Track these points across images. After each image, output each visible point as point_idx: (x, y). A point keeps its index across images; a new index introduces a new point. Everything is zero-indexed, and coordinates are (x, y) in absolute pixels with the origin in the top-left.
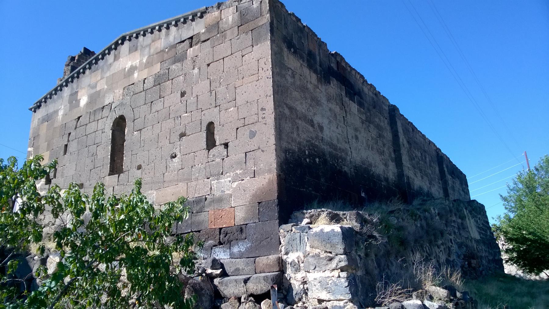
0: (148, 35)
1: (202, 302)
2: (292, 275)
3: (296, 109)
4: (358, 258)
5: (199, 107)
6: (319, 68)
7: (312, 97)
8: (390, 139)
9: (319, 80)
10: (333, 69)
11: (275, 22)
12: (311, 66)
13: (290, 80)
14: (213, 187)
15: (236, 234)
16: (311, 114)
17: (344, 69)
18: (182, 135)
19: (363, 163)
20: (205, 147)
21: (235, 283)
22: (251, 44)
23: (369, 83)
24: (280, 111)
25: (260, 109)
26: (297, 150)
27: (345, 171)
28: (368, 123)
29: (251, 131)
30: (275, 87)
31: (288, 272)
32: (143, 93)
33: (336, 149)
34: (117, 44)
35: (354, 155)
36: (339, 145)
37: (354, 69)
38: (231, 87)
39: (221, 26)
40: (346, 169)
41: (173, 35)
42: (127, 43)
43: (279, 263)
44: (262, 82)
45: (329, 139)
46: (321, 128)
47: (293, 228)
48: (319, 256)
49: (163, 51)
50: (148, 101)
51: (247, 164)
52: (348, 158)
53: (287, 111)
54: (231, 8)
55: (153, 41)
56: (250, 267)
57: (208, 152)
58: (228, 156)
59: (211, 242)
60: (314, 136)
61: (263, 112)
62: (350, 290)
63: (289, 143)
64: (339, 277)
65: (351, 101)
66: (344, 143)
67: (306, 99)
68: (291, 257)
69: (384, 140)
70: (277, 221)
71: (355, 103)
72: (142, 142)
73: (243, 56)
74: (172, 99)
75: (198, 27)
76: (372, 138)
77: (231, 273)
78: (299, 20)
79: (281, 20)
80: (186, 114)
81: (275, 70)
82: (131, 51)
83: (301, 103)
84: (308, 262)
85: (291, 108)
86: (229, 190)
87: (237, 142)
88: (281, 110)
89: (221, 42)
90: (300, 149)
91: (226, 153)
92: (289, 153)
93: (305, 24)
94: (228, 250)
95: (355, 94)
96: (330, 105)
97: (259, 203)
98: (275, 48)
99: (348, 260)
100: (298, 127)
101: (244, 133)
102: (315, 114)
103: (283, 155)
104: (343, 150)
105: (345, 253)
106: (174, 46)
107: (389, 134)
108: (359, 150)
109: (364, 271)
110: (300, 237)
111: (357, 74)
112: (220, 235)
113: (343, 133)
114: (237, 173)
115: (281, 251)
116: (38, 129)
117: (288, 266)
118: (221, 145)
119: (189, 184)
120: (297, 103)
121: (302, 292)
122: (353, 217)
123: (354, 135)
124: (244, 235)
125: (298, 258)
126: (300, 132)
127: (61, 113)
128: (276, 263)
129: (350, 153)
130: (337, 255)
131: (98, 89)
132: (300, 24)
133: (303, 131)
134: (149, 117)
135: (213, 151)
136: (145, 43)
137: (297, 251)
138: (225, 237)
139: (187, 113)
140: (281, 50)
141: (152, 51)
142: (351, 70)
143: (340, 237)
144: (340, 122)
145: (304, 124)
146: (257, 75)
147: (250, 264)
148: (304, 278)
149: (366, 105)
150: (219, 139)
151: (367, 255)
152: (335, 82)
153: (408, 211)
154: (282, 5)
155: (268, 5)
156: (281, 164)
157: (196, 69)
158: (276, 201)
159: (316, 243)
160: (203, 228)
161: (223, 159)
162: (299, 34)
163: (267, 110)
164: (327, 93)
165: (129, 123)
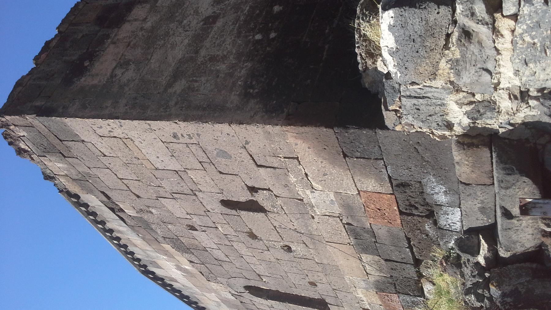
2: (503, 118)
3: (181, 62)
5: (203, 213)
11: (38, 103)
13: (130, 74)
14: (327, 214)
15: (411, 194)
16: (195, 22)
18: (253, 236)
20: (260, 215)
21: (511, 233)
22: (80, 144)
24: (176, 104)
25: (175, 140)
26: (249, 65)
29: (218, 155)
31: (496, 126)
32: (208, 266)
34: (156, 278)
38: (158, 174)
39: (76, 177)
41: (118, 227)
42: (151, 268)
43: (470, 146)
44: (133, 134)
47: (390, 108)
48: (457, 61)
49: (144, 239)
50: (216, 262)
51: (276, 165)
53: (179, 86)
54: (46, 163)
55: (136, 246)
56: (479, 193)
57: (269, 212)
58: (269, 190)
59: (428, 227)
61: (180, 136)
64: (515, 17)
68: (459, 117)
70: (380, 132)
72: (275, 276)
73: (105, 156)
74: (203, 239)
75: (94, 201)
78: (47, 43)
80: (220, 229)
81: (107, 112)
82: (159, 267)
83: (173, 47)
84: (472, 83)
85: (176, 76)
86: (328, 195)
87: (243, 176)
88: (172, 103)
89: (98, 179)
91: (265, 192)
92: (252, 87)
93: (56, 32)
94: (444, 209)
97: (345, 156)
100: (213, 59)
102: (196, 12)
103: (252, 102)
106: (132, 227)
110: (410, 97)
112: (414, 215)
114: (296, 182)
115: (443, 137)
117: (480, 123)
118: (252, 195)
119: (327, 240)
124: (412, 183)
125: (460, 104)
126: (220, 53)
128: (470, 152)
130: (455, 22)
131: (219, 301)
132: (54, 44)
133: (220, 45)
134: (238, 265)
135: (266, 205)
136: (142, 253)
137: (443, 105)
138: (417, 208)
139: (217, 228)
141: (148, 248)
145: (207, 43)
146: (124, 140)
147: (472, 192)
148: (512, 97)
150: (244, 197)
155: (13, 117)
157: (150, 209)
159: (425, 68)
161: (276, 196)
163: (175, 131)
165: (252, 283)
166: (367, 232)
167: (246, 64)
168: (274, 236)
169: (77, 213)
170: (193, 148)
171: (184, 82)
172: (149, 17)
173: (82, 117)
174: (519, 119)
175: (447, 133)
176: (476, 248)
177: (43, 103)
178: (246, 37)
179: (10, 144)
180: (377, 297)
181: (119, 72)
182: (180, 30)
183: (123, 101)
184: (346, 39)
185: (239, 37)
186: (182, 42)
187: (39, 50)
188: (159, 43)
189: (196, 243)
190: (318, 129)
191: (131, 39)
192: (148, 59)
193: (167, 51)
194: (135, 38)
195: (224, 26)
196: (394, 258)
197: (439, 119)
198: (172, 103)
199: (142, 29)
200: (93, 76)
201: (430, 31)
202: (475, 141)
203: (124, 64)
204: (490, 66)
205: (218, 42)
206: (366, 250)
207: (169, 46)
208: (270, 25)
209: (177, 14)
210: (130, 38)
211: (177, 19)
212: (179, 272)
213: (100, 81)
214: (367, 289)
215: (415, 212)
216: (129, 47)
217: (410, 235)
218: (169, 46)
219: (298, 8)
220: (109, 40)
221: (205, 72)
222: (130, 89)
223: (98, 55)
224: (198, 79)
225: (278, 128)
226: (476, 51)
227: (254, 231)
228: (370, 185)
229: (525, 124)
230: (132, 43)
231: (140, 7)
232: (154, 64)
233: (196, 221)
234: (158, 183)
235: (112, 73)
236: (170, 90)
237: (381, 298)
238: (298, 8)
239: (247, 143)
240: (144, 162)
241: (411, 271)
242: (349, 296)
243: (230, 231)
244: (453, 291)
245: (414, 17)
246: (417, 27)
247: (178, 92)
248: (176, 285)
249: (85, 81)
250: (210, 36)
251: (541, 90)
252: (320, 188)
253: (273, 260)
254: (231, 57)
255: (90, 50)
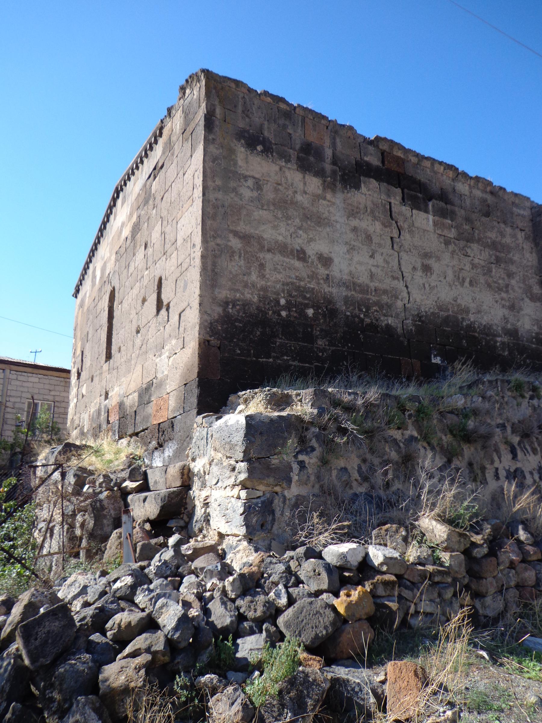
0: (132, 178)
1: (102, 525)
3: (260, 239)
4: (295, 467)
6: (328, 167)
7: (304, 214)
8: (530, 264)
9: (329, 186)
10: (368, 164)
11: (218, 111)
12: (304, 166)
17: (401, 162)
18: (144, 300)
19: (440, 308)
23: (472, 174)
24: (218, 245)
26: (256, 299)
27: (388, 325)
28: (462, 243)
29: (185, 281)
30: (210, 210)
31: (194, 488)
33: (364, 289)
34: (114, 200)
35: (417, 295)
36: (372, 285)
37: (428, 159)
40: (390, 321)
42: (121, 195)
43: (182, 474)
45: (345, 277)
46: (326, 261)
49: (139, 194)
50: (127, 264)
52: (399, 304)
53: (235, 243)
58: (168, 321)
60: (304, 275)
61: (194, 250)
62: (245, 519)
63: (237, 290)
65: (414, 211)
66: (388, 281)
67: (290, 219)
68: (197, 466)
69: (513, 268)
70: (196, 412)
71: (426, 211)
76: (474, 266)
77: (153, 486)
78: (282, 100)
79: (235, 106)
81: (210, 183)
83: (275, 227)
85: (246, 238)
87: (175, 300)
88: (219, 241)
90: (263, 299)
92: (234, 306)
93: (295, 105)
95: (430, 200)
96: (355, 222)
97: (185, 385)
98: (215, 150)
99: (250, 471)
100: (262, 266)
101: (181, 284)
102: (310, 240)
103: (220, 310)
104: (385, 292)
105: (247, 458)
107: (528, 255)
108: (432, 288)
109: (317, 486)
110: (207, 434)
111: (437, 166)
113: (388, 263)
115: (188, 456)
116: (77, 317)
117: (196, 479)
120: (263, 227)
121: (202, 519)
122: (309, 398)
123: (419, 265)
125: (204, 467)
127: (88, 295)
128: (179, 474)
129: (405, 295)
130: (237, 462)
132: (282, 106)
133: (275, 269)
134: (127, 284)
136: (131, 189)
140: (232, 151)
142: (419, 161)
143: (242, 433)
144: (380, 245)
145: (278, 258)
149: (461, 213)
151: (324, 462)
152: (374, 183)
153: (509, 382)
154: (237, 83)
156: (211, 323)
158: (197, 379)
160: (149, 425)
162: (281, 122)
164: (349, 204)
166: (149, 398)
167: (256, 297)
168: (144, 321)
169: (148, 135)
170: (188, 260)
171: (240, 246)
172: (307, 196)
173: (204, 161)
174: (197, 503)
175: (190, 458)
176: (133, 479)
177: (218, 116)
178: (283, 291)
179: (187, 81)
180: (116, 403)
181: (250, 183)
182: (292, 230)
183: (220, 195)
184: (254, 383)
185: (283, 285)
186: (279, 234)
187: (275, 94)
188: (279, 212)
189: (138, 247)
190: (197, 366)
191: (284, 185)
192: (262, 206)
193: (270, 222)
194: (286, 188)
195: (294, 269)
196: (137, 418)
197: (196, 453)
198: (219, 241)
199: (296, 192)
200: (247, 158)
201: (232, 447)
202: (185, 476)
203: (258, 186)
204: (219, 484)
205: (279, 267)
206: (140, 396)
207: (276, 223)
208: (294, 309)
209: (309, 223)
210: (286, 183)
211: (304, 224)
212: (120, 224)
213: (240, 167)
214: (119, 395)
215: (161, 434)
216: (275, 185)
217: (149, 430)
218: (276, 223)
219: (309, 329)
220: (284, 164)
221: (248, 262)
222: (232, 198)
223: (268, 156)
224: (242, 258)
225: (197, 335)
226: (226, 475)
227: (146, 303)
228: (172, 403)
229: (194, 507)
230: (280, 187)
231: (319, 184)
232: (258, 214)
233: (150, 250)
234: (170, 221)
235: (249, 176)
236: (231, 236)
237: (115, 406)
238: (309, 329)
239: (191, 308)
240: (180, 212)
241: (130, 431)
242: (115, 380)
243: (145, 281)
244: (116, 463)
245: (239, 437)
246: (235, 439)
247: (230, 244)
248: (112, 217)
249: (241, 152)
250: (285, 259)
251: (209, 515)
252: (170, 364)
253: (132, 316)
254: (263, 283)
255: (274, 147)
